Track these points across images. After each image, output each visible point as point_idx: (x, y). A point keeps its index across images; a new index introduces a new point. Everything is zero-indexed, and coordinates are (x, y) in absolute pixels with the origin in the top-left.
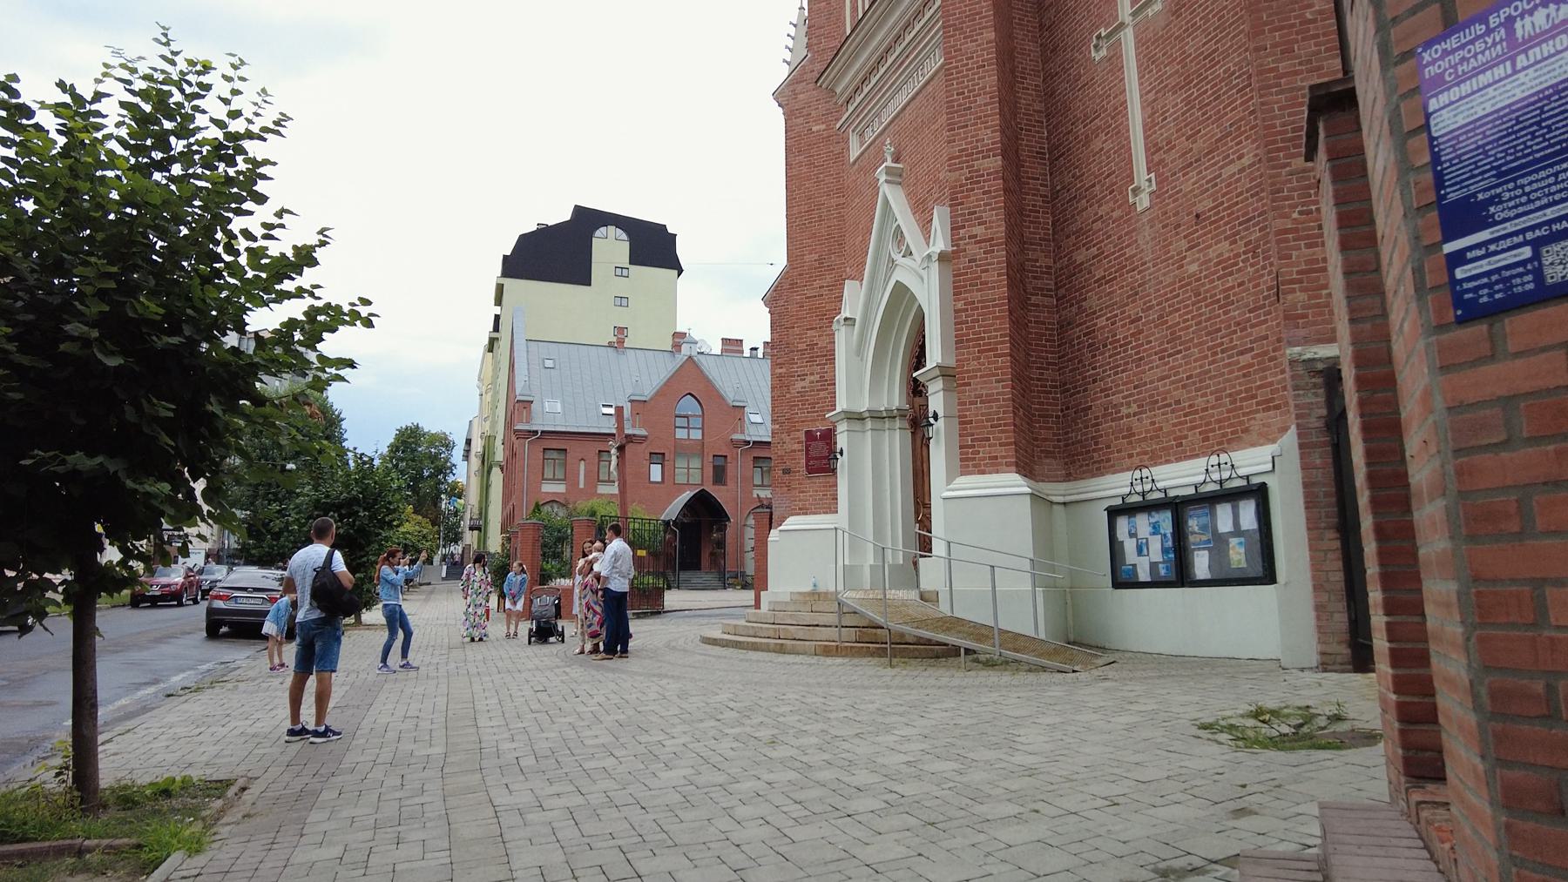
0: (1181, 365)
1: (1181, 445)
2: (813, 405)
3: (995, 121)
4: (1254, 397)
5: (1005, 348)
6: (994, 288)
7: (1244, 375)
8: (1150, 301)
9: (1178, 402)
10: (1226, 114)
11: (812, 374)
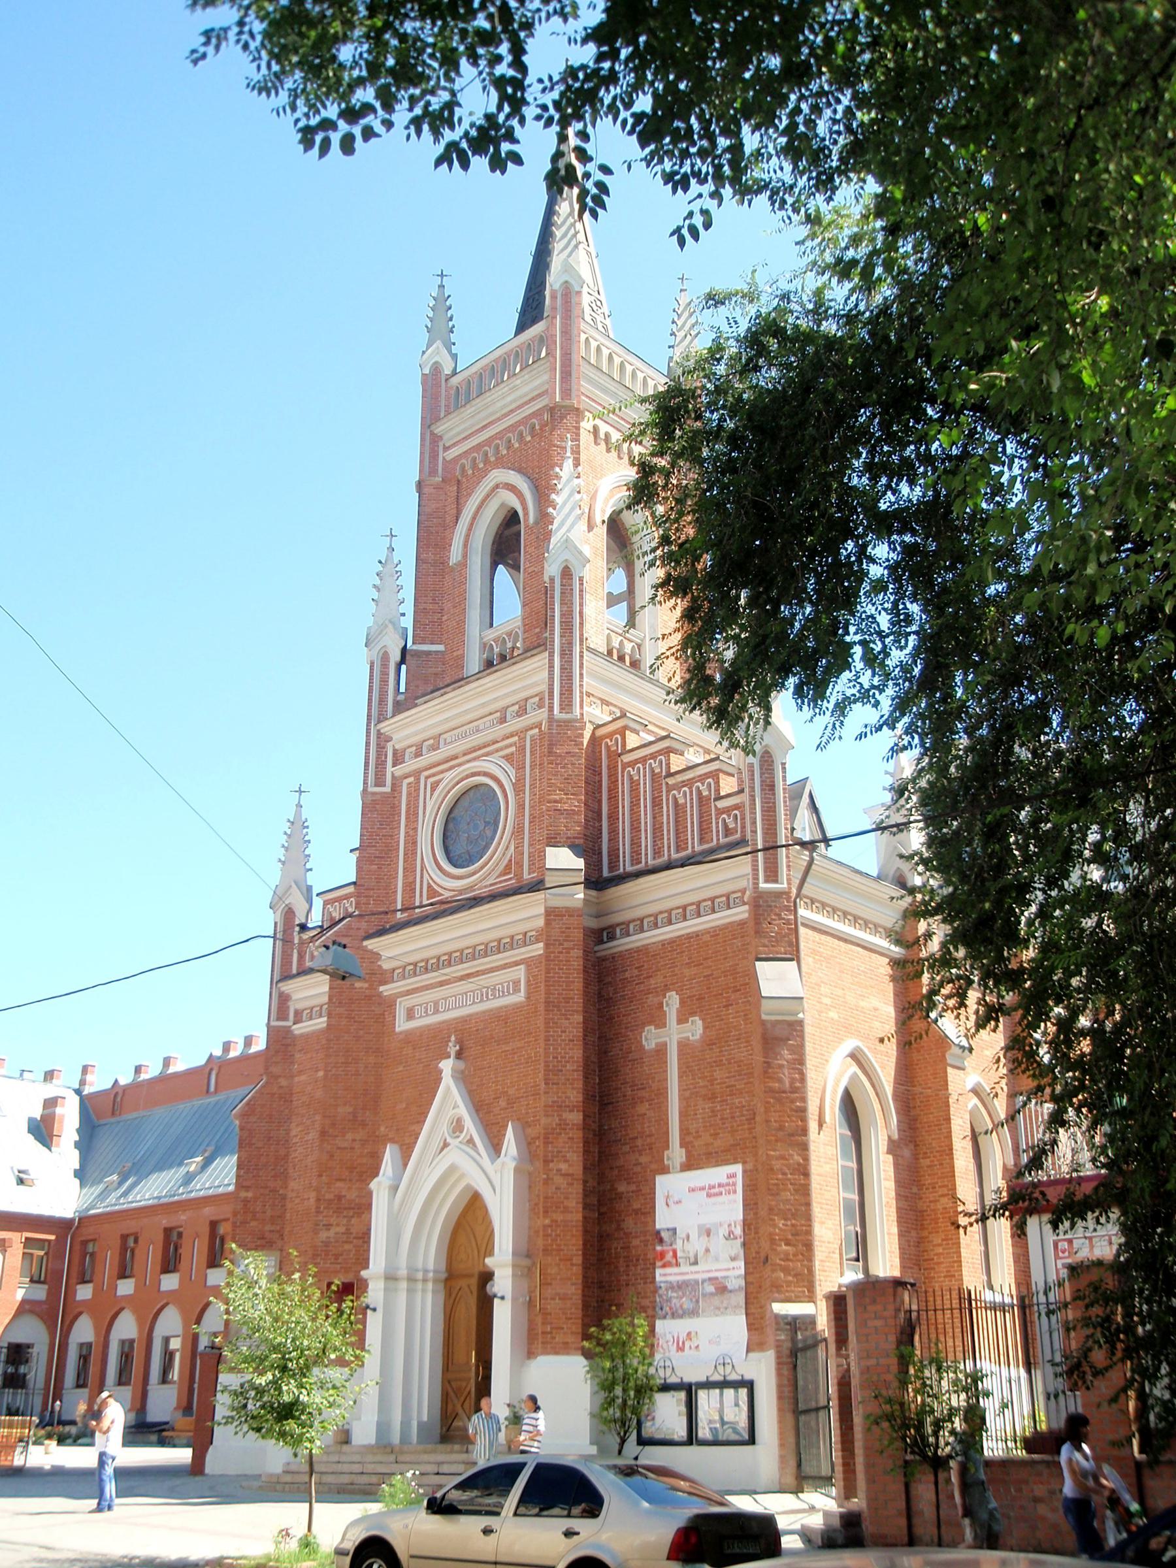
2: (337, 1256)
3: (579, 1085)
5: (578, 1260)
11: (338, 1225)
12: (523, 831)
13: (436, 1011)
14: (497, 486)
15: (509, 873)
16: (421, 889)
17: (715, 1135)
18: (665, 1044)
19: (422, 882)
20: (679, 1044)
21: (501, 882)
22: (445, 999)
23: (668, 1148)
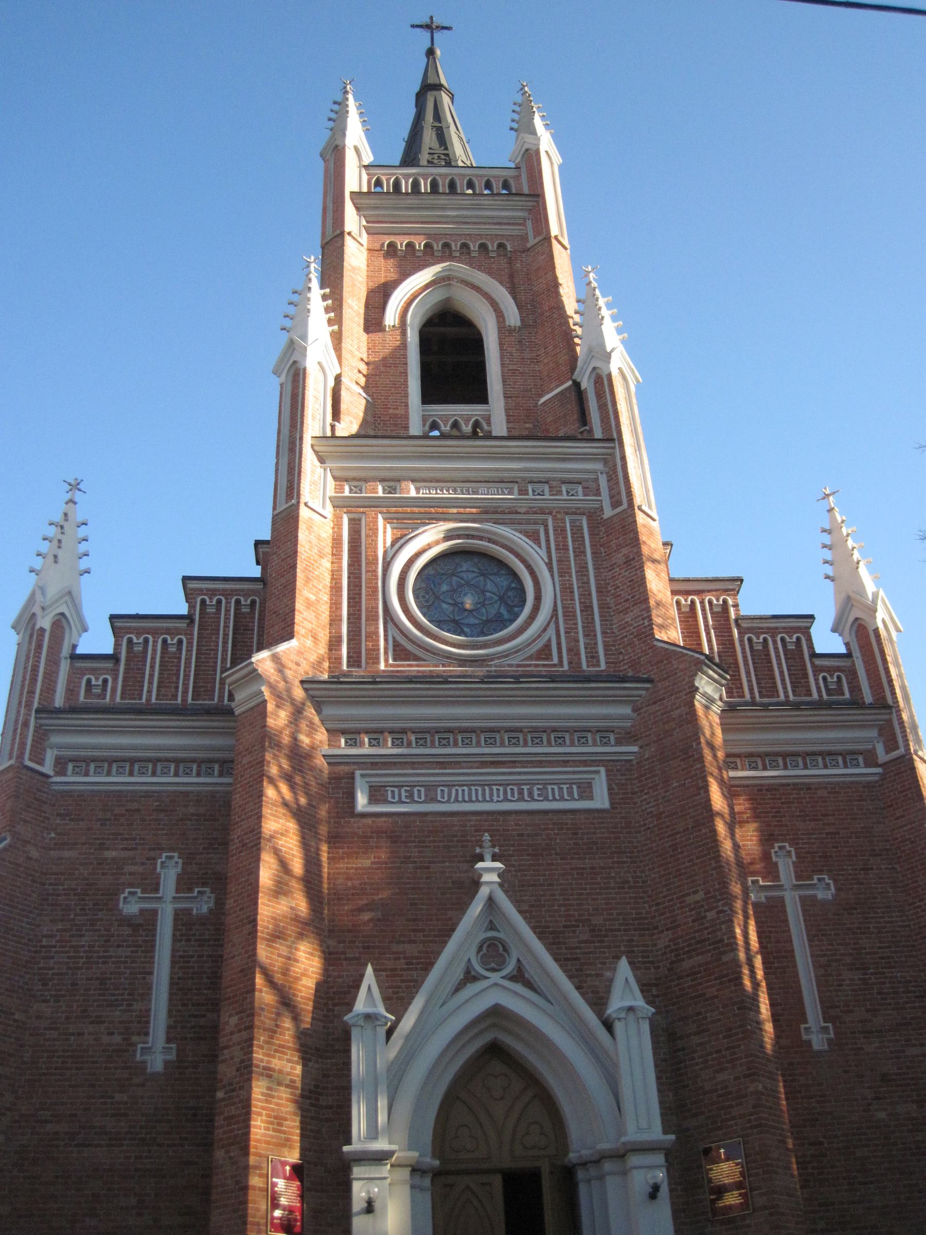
12: (575, 616)
13: (433, 800)
15: (547, 659)
18: (782, 900)
20: (803, 899)
21: (536, 666)
22: (450, 786)
23: (806, 1022)
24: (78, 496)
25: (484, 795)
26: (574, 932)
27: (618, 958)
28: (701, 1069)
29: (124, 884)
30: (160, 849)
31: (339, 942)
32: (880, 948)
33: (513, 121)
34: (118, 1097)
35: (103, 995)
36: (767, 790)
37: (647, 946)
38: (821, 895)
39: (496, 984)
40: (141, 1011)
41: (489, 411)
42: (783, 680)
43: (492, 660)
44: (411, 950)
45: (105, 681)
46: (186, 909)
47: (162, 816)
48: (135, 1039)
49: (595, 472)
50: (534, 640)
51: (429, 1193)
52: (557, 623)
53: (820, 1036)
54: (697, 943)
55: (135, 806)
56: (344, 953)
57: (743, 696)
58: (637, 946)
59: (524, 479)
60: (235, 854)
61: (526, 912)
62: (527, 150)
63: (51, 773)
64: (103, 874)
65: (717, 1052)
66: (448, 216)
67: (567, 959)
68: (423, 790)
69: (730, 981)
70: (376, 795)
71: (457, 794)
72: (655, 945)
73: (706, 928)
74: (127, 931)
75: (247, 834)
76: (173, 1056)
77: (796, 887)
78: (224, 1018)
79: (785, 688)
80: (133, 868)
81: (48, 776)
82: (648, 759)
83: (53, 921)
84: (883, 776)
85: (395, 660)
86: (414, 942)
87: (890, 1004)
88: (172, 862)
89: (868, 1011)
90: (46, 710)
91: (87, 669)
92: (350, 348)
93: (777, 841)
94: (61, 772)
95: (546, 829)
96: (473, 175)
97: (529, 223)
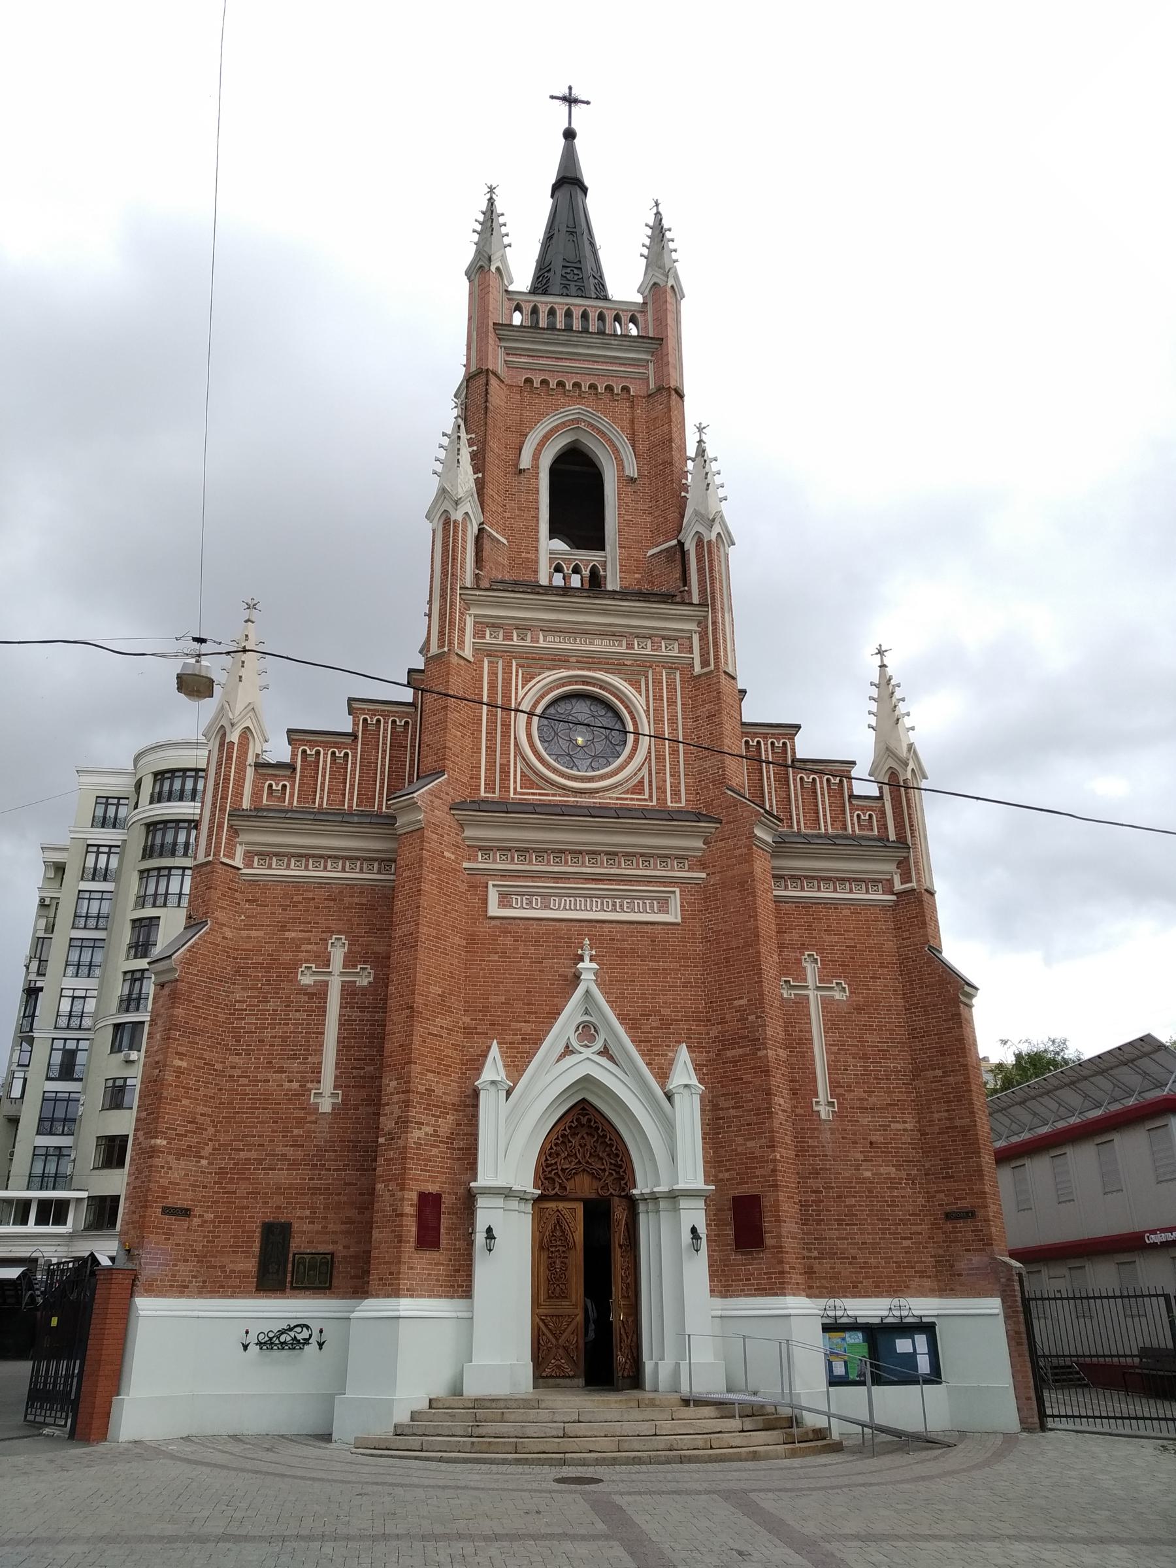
0: (857, 1234)
1: (854, 1287)
4: (912, 1267)
6: (789, 1149)
7: (906, 1253)
8: (831, 1183)
9: (854, 1258)
10: (895, 1092)
11: (427, 1125)
12: (665, 759)
13: (547, 907)
14: (578, 421)
15: (640, 794)
16: (515, 775)
17: (870, 1092)
18: (807, 997)
19: (515, 767)
24: (255, 615)
25: (586, 905)
26: (648, 1020)
27: (679, 1042)
28: (735, 1136)
29: (301, 960)
30: (329, 932)
31: (472, 1020)
32: (879, 1042)
33: (644, 245)
34: (296, 1131)
35: (285, 1050)
36: (803, 907)
37: (702, 1034)
38: (838, 995)
39: (588, 1058)
40: (314, 1063)
41: (606, 557)
42: (825, 815)
43: (598, 793)
44: (526, 1028)
45: (284, 786)
46: (350, 982)
47: (332, 904)
48: (309, 1085)
49: (690, 631)
50: (631, 777)
51: (530, 1216)
52: (650, 763)
53: (827, 1108)
54: (740, 1038)
55: (310, 895)
56: (476, 1029)
57: (792, 827)
58: (694, 1034)
59: (631, 634)
60: (396, 951)
61: (613, 1001)
62: (655, 284)
63: (241, 866)
64: (284, 951)
65: (748, 1125)
66: (580, 354)
67: (640, 1041)
68: (539, 898)
69: (761, 1072)
70: (505, 899)
71: (565, 904)
72: (709, 1034)
73: (747, 1028)
74: (304, 998)
75: (405, 935)
76: (339, 1101)
77: (818, 988)
78: (385, 1081)
79: (825, 822)
80: (309, 947)
81: (239, 869)
82: (713, 885)
83: (242, 989)
84: (896, 903)
85: (521, 788)
86: (529, 1022)
87: (883, 1088)
88: (339, 944)
89: (865, 1091)
90: (236, 813)
91: (269, 775)
92: (491, 492)
93: (807, 949)
94: (249, 865)
95: (632, 936)
96: (603, 308)
97: (651, 366)
